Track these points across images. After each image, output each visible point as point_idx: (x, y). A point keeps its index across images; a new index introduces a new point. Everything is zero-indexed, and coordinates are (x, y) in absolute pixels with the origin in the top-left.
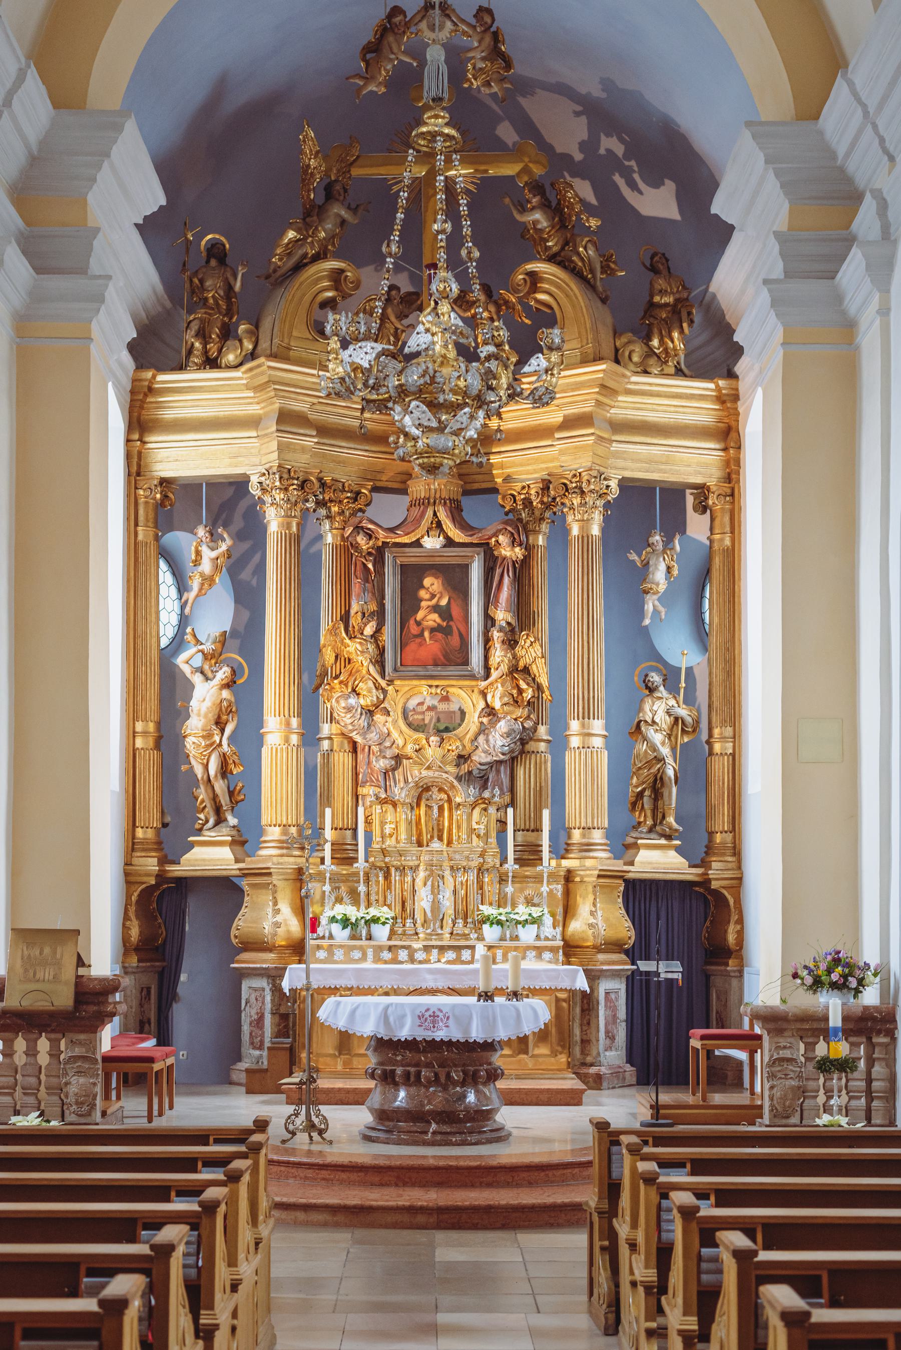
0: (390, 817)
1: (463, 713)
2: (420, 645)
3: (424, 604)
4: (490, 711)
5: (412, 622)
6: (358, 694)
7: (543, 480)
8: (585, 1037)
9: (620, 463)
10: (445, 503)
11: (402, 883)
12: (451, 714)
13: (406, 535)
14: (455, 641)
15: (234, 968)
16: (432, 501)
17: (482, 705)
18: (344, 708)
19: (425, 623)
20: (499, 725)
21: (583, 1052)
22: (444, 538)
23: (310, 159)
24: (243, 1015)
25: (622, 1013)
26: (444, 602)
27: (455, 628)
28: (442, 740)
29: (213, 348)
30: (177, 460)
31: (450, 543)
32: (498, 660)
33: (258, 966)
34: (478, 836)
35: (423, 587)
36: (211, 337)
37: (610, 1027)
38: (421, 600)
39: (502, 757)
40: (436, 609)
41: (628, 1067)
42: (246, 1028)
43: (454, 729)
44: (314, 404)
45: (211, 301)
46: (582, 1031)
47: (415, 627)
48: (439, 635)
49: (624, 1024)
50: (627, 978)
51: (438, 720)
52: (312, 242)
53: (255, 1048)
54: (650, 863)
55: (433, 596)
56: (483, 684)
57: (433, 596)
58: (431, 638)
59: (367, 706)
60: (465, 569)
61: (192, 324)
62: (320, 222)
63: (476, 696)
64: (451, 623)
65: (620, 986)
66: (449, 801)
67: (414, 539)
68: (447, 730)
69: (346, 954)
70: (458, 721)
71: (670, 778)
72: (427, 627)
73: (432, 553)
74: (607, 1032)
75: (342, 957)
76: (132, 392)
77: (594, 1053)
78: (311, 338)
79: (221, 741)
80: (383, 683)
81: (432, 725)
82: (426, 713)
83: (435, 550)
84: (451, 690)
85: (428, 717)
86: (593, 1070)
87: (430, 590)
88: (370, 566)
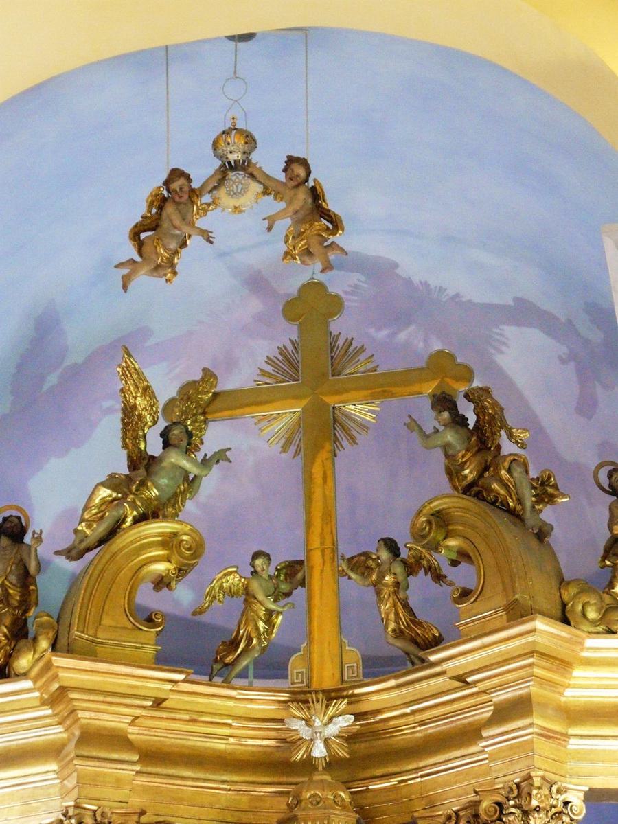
9: (584, 766)
23: (135, 398)
44: (137, 717)
52: (134, 501)
78: (130, 626)
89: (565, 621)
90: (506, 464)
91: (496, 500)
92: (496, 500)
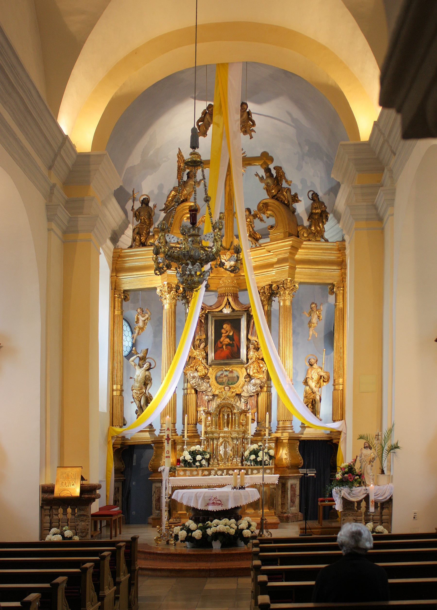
0: (209, 418)
1: (238, 377)
2: (222, 351)
3: (223, 335)
4: (249, 376)
5: (219, 342)
6: (198, 371)
7: (270, 285)
8: (283, 502)
10: (232, 295)
11: (213, 444)
12: (233, 378)
13: (217, 308)
14: (235, 349)
15: (150, 479)
16: (227, 294)
17: (245, 374)
18: (192, 377)
19: (224, 343)
20: (252, 381)
21: (282, 508)
22: (231, 308)
24: (153, 497)
25: (298, 492)
26: (231, 334)
27: (235, 344)
28: (230, 388)
29: (143, 239)
30: (129, 283)
31: (233, 310)
32: (251, 356)
33: (158, 478)
34: (243, 425)
35: (223, 328)
36: (142, 234)
37: (292, 498)
38: (222, 333)
39: (253, 394)
40: (228, 337)
41: (300, 513)
42: (154, 502)
43: (235, 384)
45: (143, 220)
46: (282, 500)
47: (220, 344)
48: (229, 347)
49: (298, 497)
50: (300, 479)
51: (229, 380)
53: (157, 510)
54: (310, 434)
55: (227, 332)
56: (246, 366)
57: (227, 332)
58: (226, 348)
59: (201, 376)
60: (239, 320)
61: (135, 230)
62: (185, 187)
63: (244, 370)
64: (234, 342)
65: (297, 482)
66: (231, 412)
67: (220, 310)
68: (232, 384)
69: (191, 473)
70: (236, 380)
71: (318, 400)
72: (225, 344)
73: (227, 315)
74: (291, 500)
75: (189, 474)
76: (113, 257)
77: (286, 508)
79: (145, 392)
80: (207, 366)
81: (226, 382)
82: (224, 378)
83: (227, 314)
84: (234, 368)
85: (225, 379)
86: (285, 515)
87: (226, 329)
88: (203, 321)
89: (298, 237)
90: (285, 191)
91: (282, 201)
92: (282, 201)
